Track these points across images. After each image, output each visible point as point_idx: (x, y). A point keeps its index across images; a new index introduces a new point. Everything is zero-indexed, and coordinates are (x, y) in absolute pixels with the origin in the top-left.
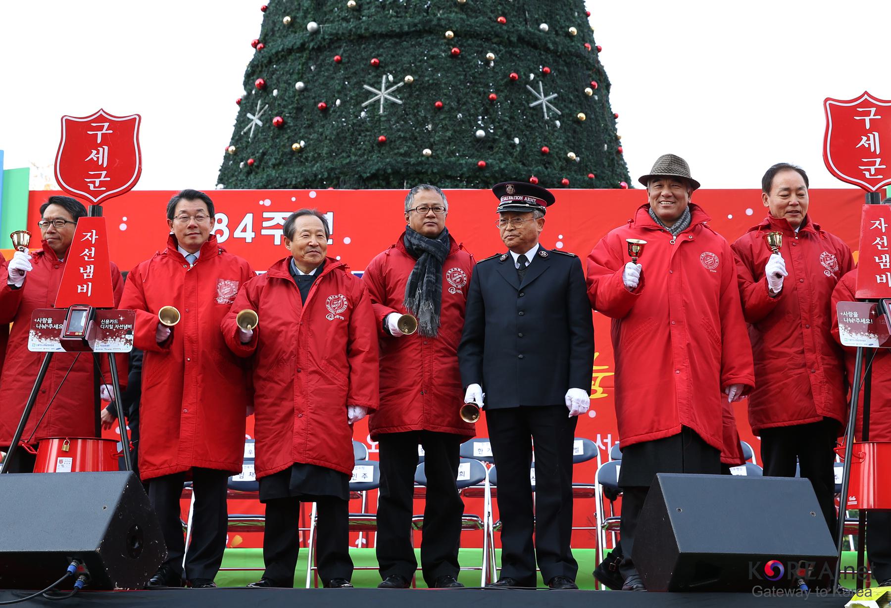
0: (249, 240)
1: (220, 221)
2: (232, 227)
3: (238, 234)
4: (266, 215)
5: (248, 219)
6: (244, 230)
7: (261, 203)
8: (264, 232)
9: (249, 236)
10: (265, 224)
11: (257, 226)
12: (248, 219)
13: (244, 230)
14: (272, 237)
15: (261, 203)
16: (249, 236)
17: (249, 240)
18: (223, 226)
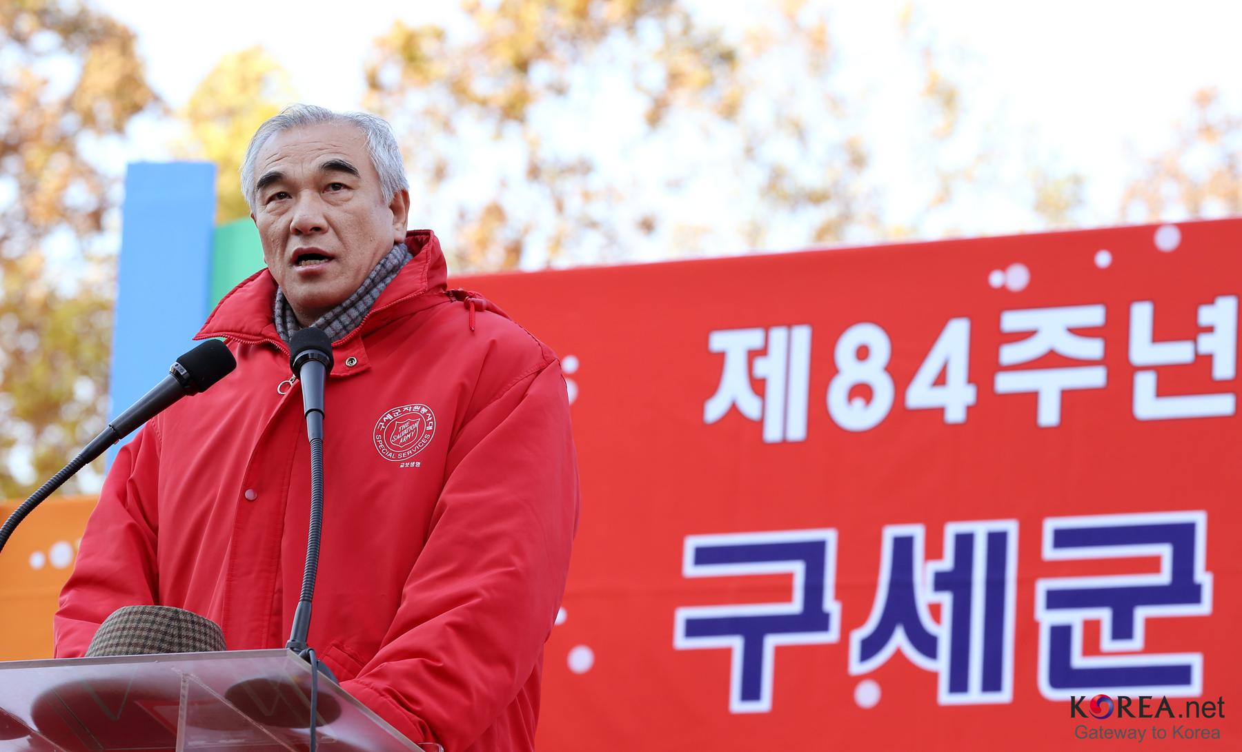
0: (955, 414)
1: (863, 353)
2: (902, 370)
3: (920, 395)
4: (1012, 321)
5: (955, 340)
6: (941, 380)
7: (996, 279)
8: (1006, 383)
9: (956, 400)
10: (1010, 354)
11: (983, 366)
12: (955, 340)
13: (941, 380)
14: (1030, 400)
15: (996, 279)
16: (956, 400)
17: (955, 414)
18: (875, 372)
